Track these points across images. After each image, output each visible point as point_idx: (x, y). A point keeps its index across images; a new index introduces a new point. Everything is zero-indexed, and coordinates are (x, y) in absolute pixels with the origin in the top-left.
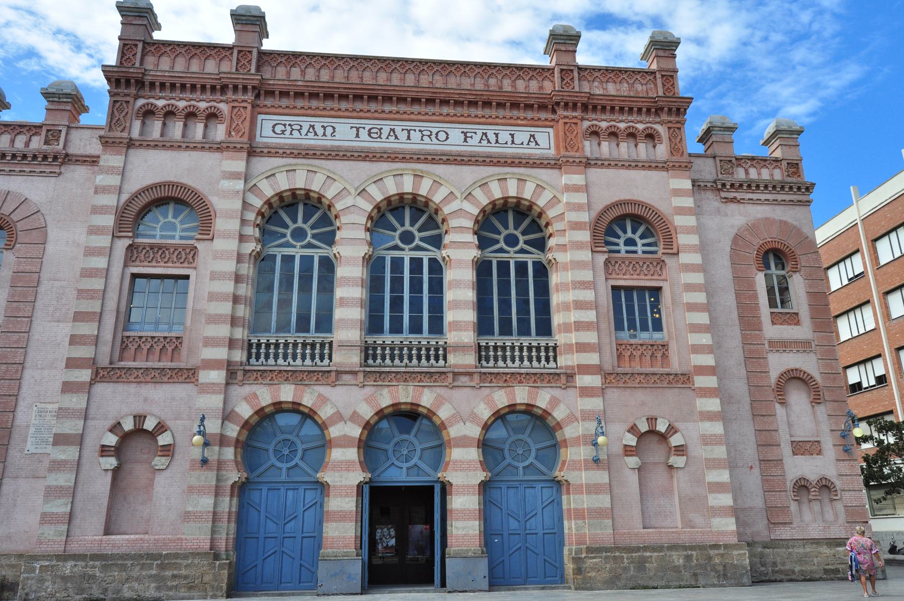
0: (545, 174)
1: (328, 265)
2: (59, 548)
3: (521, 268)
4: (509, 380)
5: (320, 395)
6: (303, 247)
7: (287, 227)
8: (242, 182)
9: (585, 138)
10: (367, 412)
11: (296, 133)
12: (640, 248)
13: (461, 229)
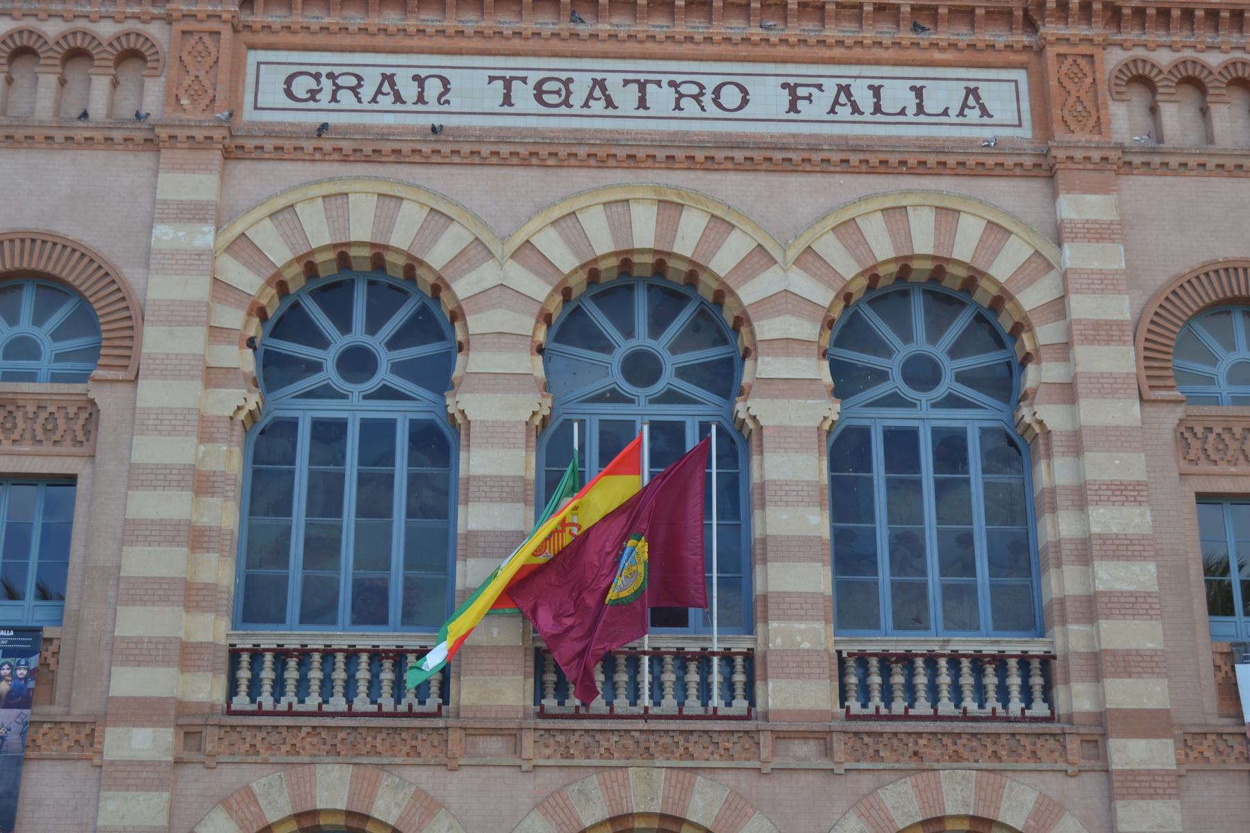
1: (437, 443)
3: (951, 449)
5: (419, 794)
7: (323, 343)
8: (209, 228)
9: (1118, 97)
11: (346, 98)
13: (788, 346)
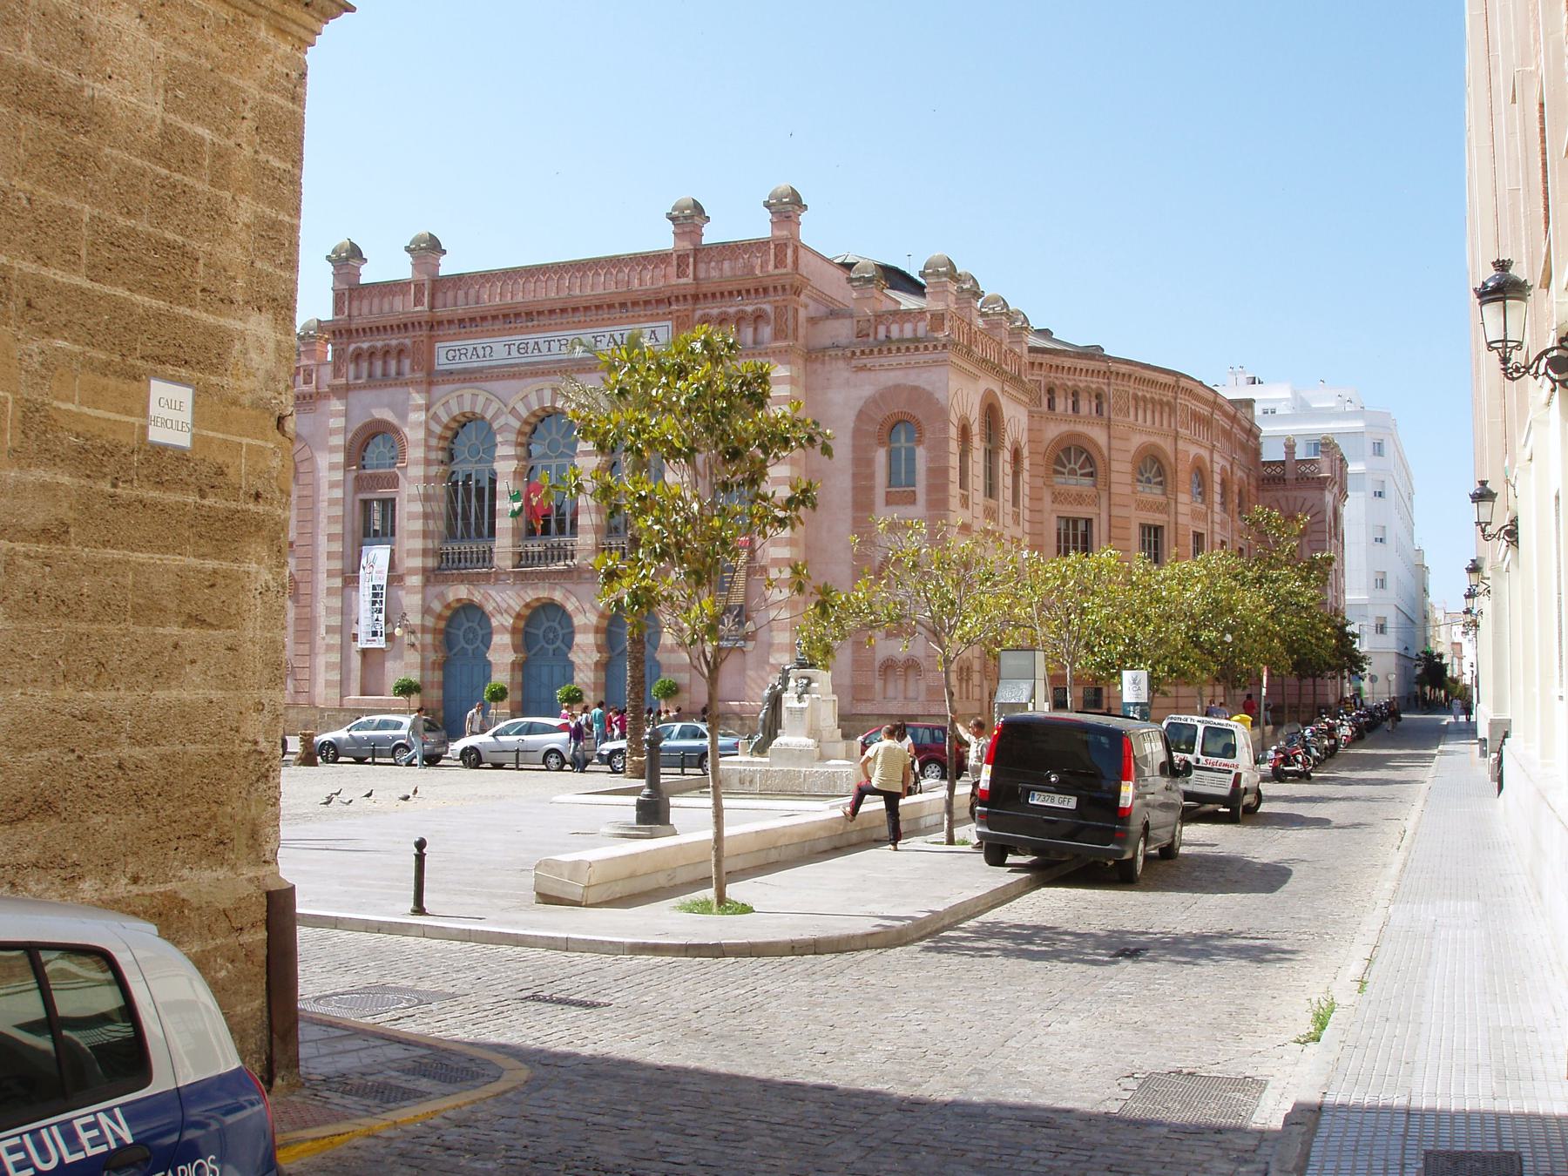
10: (517, 607)
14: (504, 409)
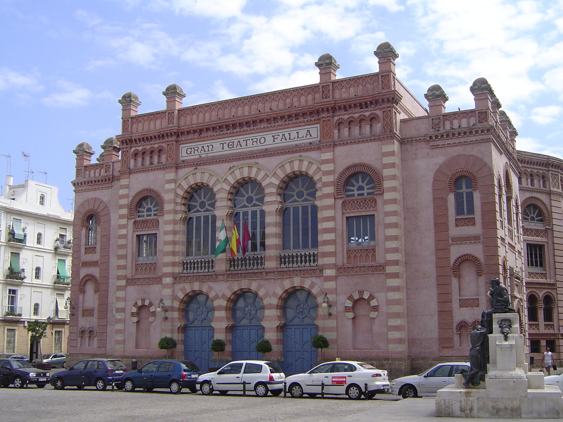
0: (313, 155)
2: (122, 354)
4: (291, 273)
6: (204, 211)
10: (229, 294)
12: (365, 192)
13: (271, 194)
14: (221, 179)
